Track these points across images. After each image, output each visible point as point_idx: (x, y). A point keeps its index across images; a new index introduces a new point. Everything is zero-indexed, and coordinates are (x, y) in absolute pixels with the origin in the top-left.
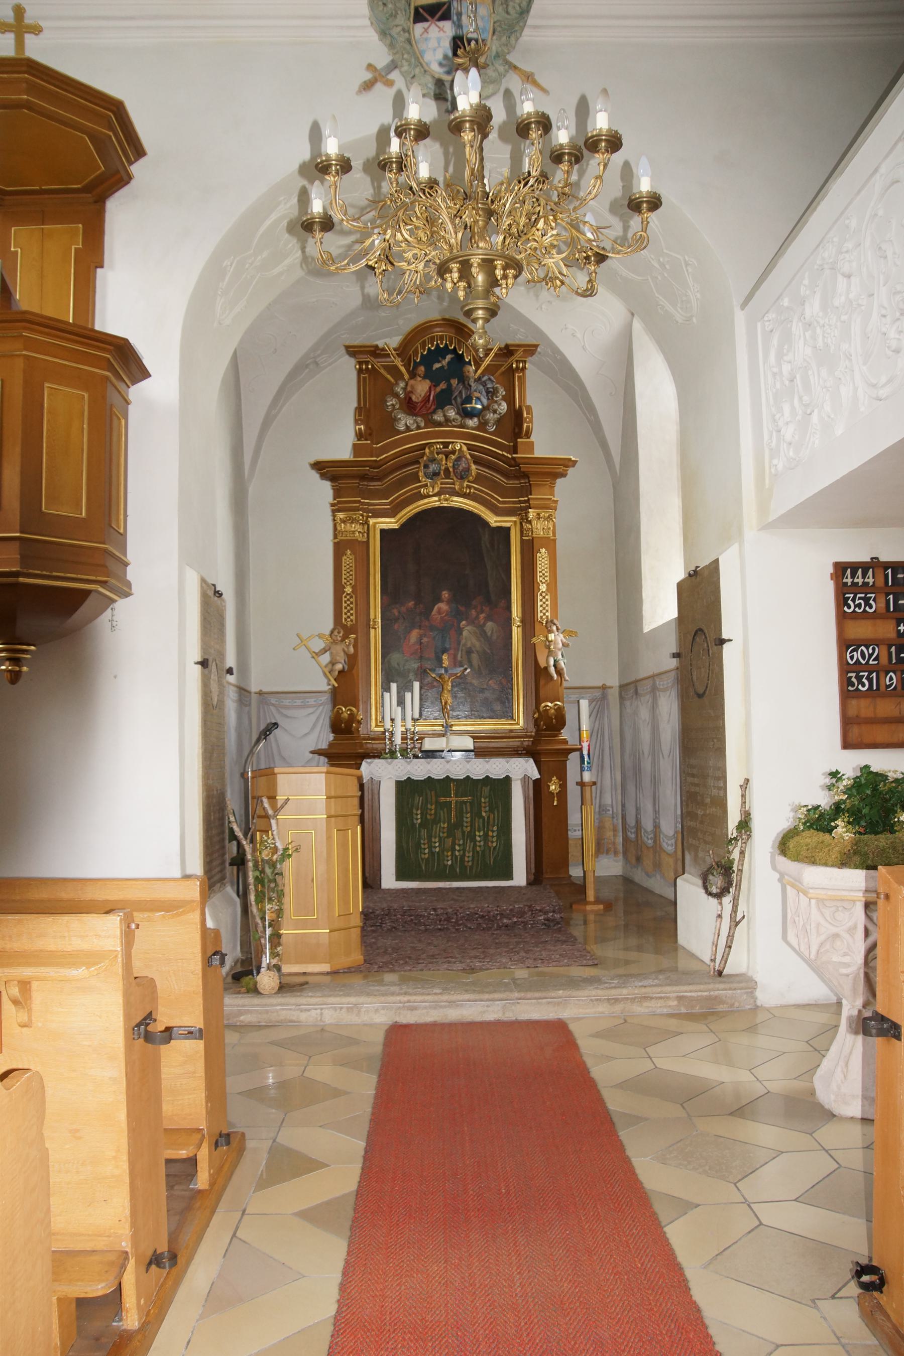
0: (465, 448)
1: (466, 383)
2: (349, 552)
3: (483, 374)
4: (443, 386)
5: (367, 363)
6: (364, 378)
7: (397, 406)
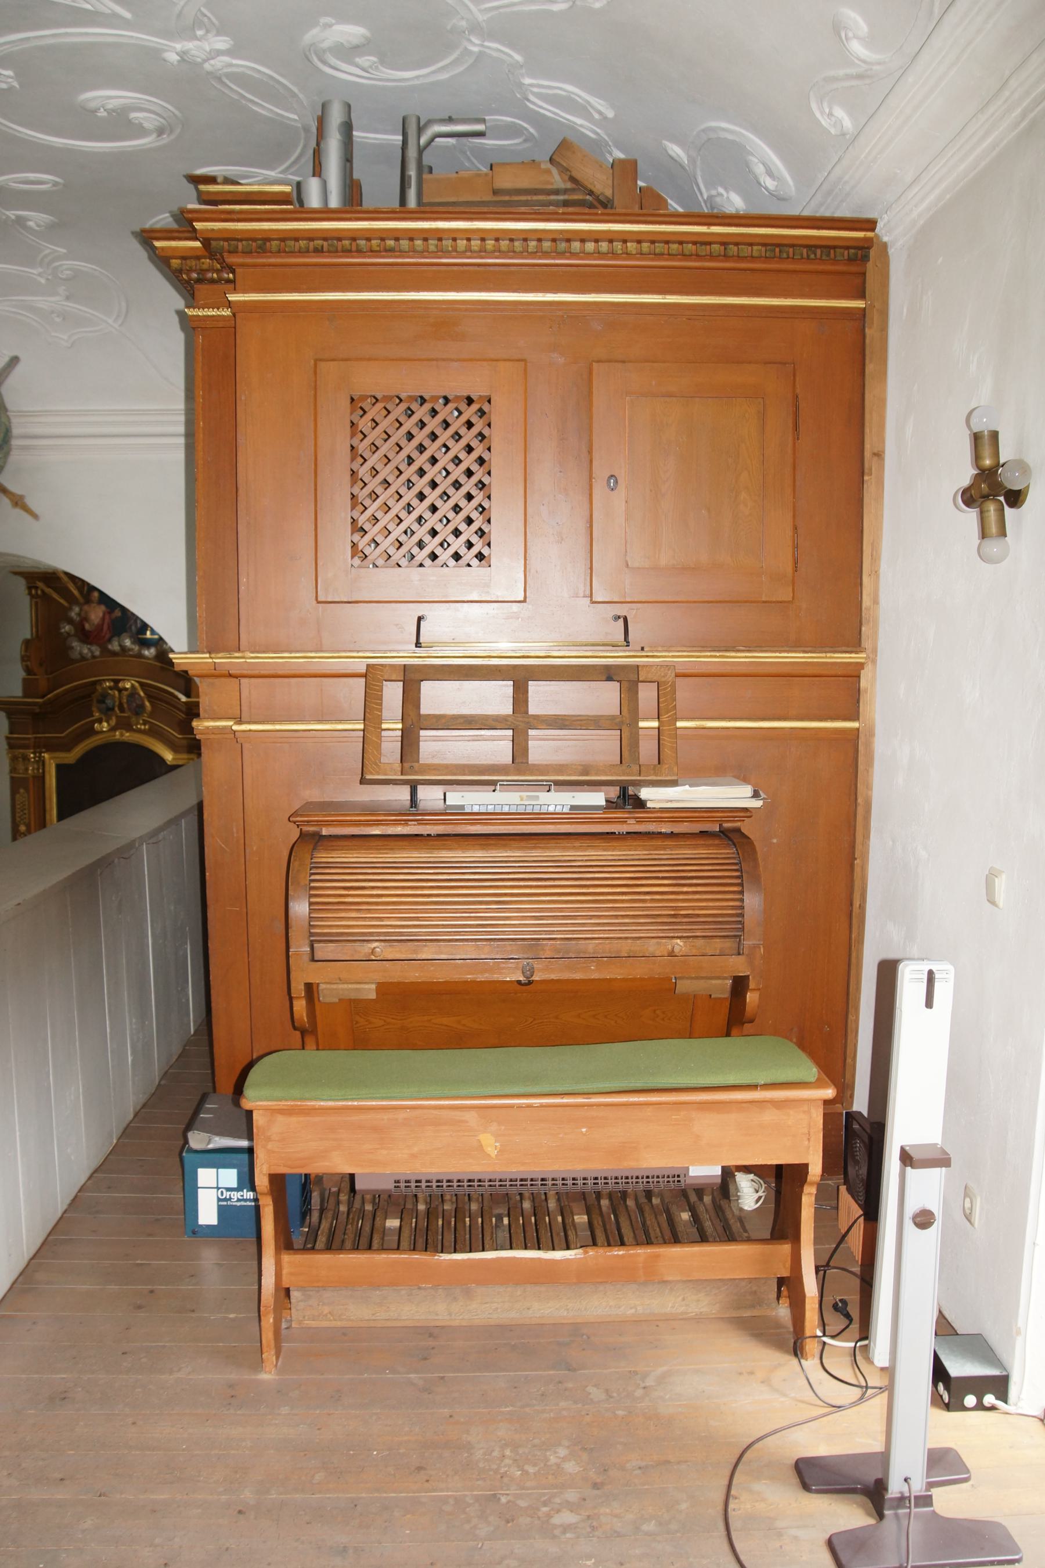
0: (137, 685)
2: (22, 791)
6: (36, 603)
7: (73, 632)
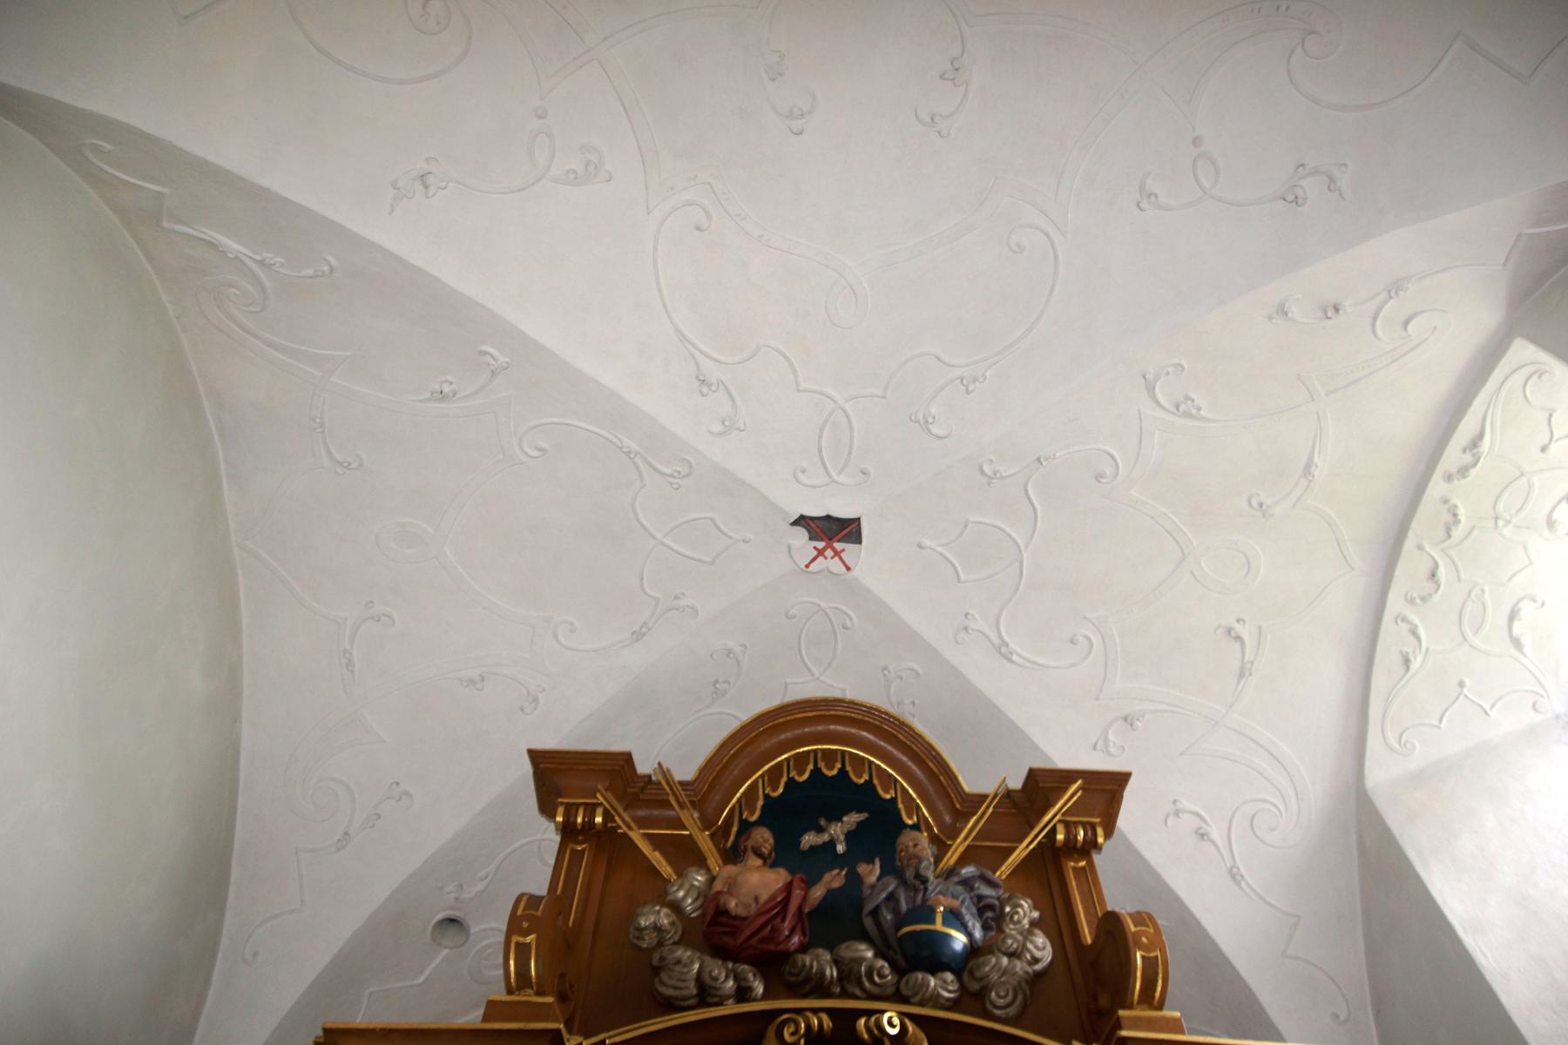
1: (909, 874)
3: (963, 860)
4: (834, 879)
5: (591, 809)
